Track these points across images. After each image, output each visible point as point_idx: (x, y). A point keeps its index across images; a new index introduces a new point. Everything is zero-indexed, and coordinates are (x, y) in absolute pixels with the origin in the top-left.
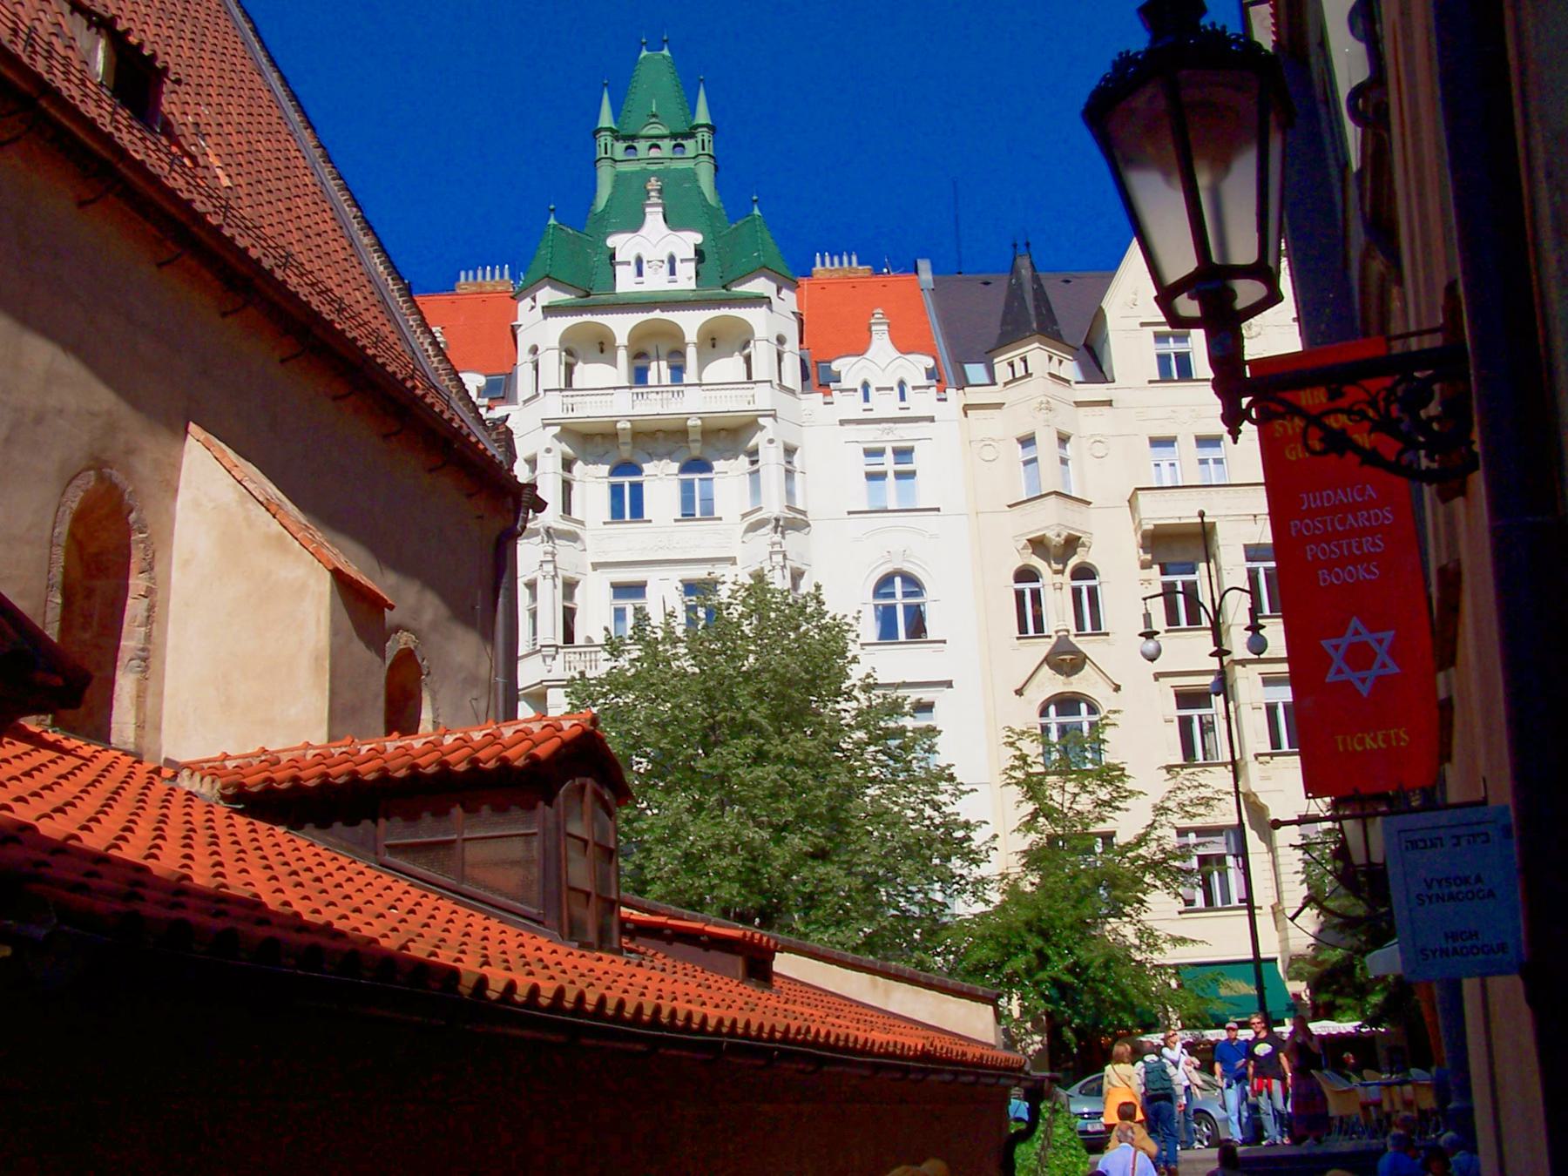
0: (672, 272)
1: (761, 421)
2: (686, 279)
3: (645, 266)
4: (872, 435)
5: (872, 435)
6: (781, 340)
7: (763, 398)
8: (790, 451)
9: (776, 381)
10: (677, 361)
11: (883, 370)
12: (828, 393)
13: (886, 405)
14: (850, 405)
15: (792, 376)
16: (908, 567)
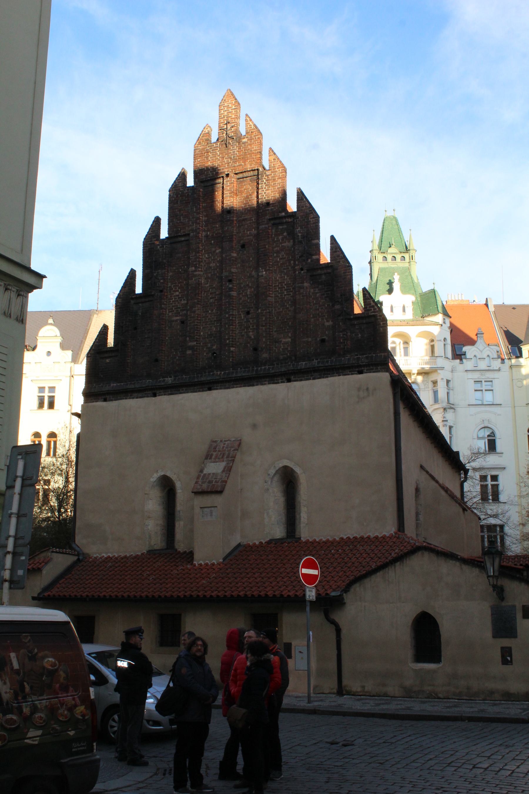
0: (404, 310)
1: (439, 371)
2: (409, 315)
3: (394, 309)
4: (476, 376)
5: (476, 376)
6: (445, 339)
7: (440, 362)
8: (448, 381)
9: (444, 356)
10: (406, 346)
11: (481, 352)
12: (461, 359)
13: (483, 365)
14: (468, 364)
15: (449, 354)
16: (490, 426)
